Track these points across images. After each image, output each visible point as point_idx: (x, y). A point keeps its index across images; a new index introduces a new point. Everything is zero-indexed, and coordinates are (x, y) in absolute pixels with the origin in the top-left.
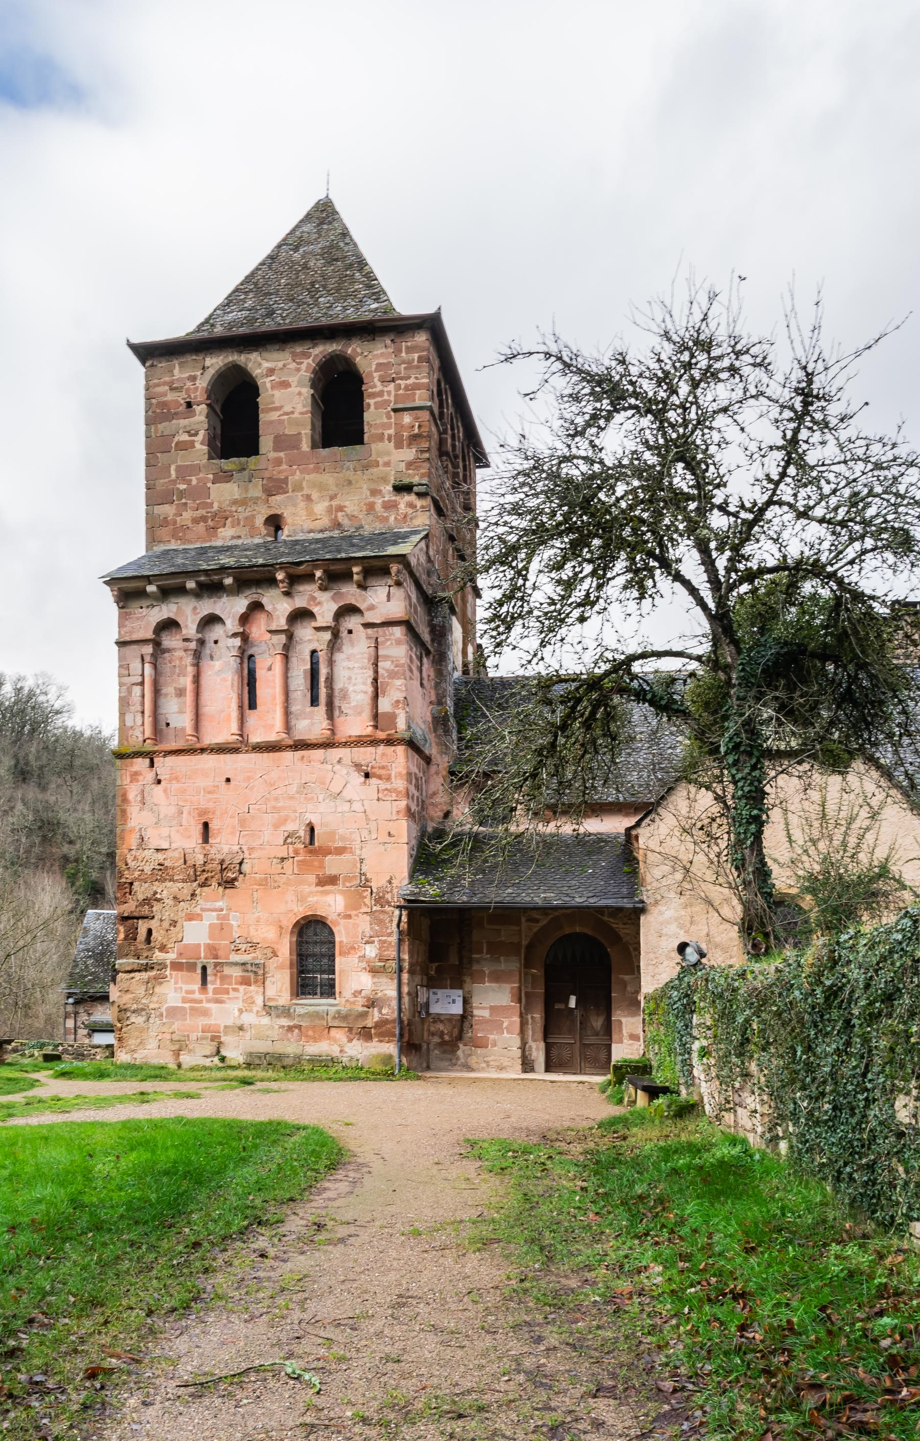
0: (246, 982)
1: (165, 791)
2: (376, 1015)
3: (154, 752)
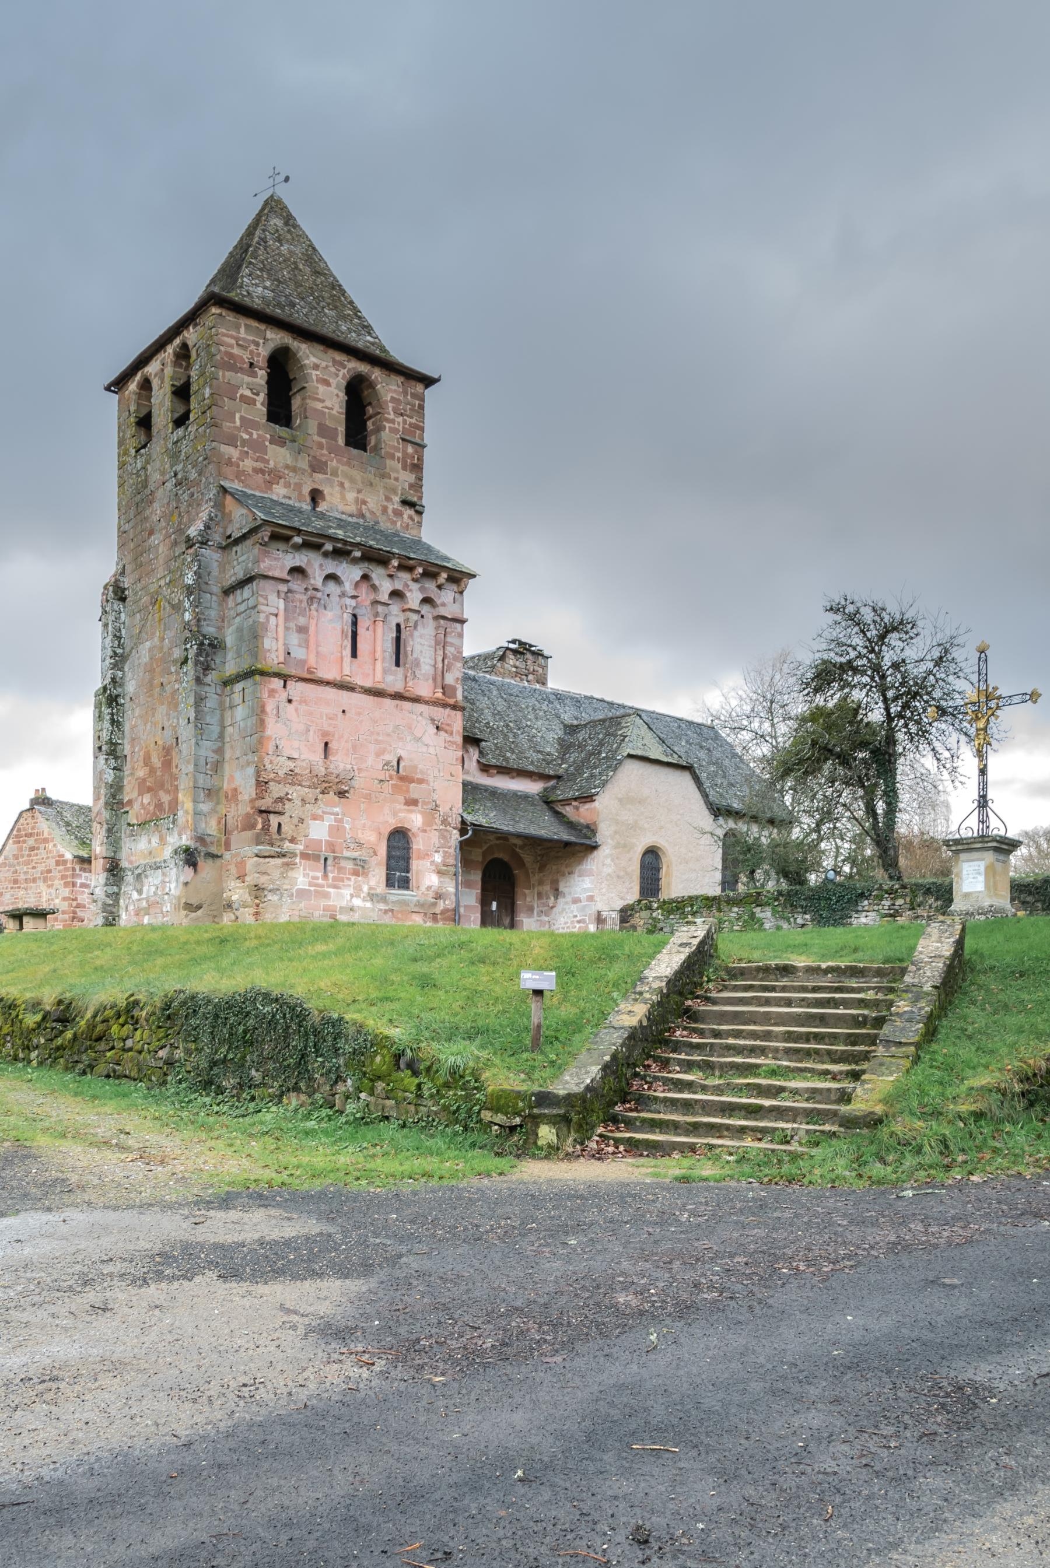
0: (356, 873)
1: (296, 710)
2: (441, 905)
3: (290, 676)
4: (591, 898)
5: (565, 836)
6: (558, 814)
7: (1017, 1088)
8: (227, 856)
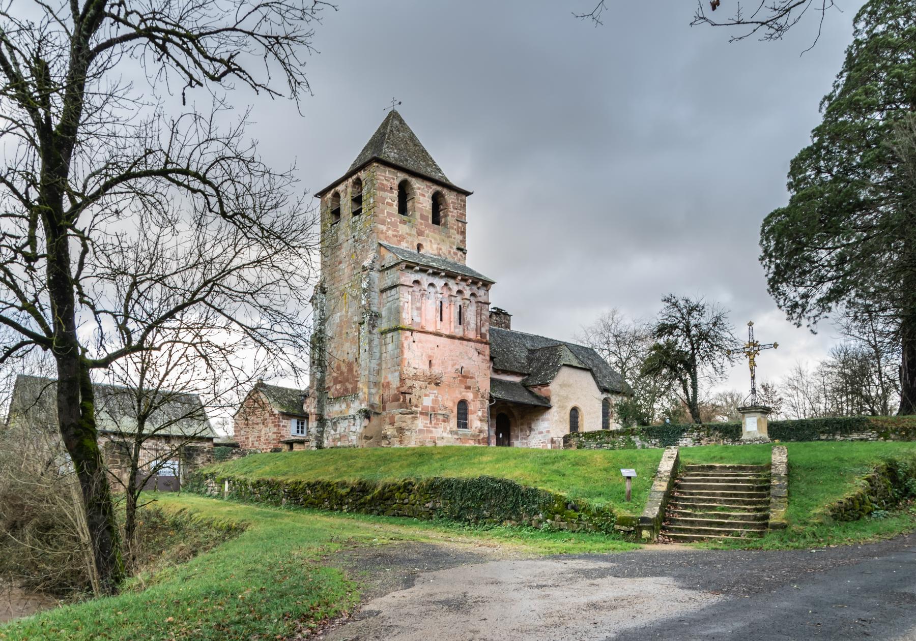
0: (444, 421)
2: (482, 436)
4: (548, 432)
5: (536, 402)
6: (531, 392)
7: (831, 514)
8: (384, 413)
